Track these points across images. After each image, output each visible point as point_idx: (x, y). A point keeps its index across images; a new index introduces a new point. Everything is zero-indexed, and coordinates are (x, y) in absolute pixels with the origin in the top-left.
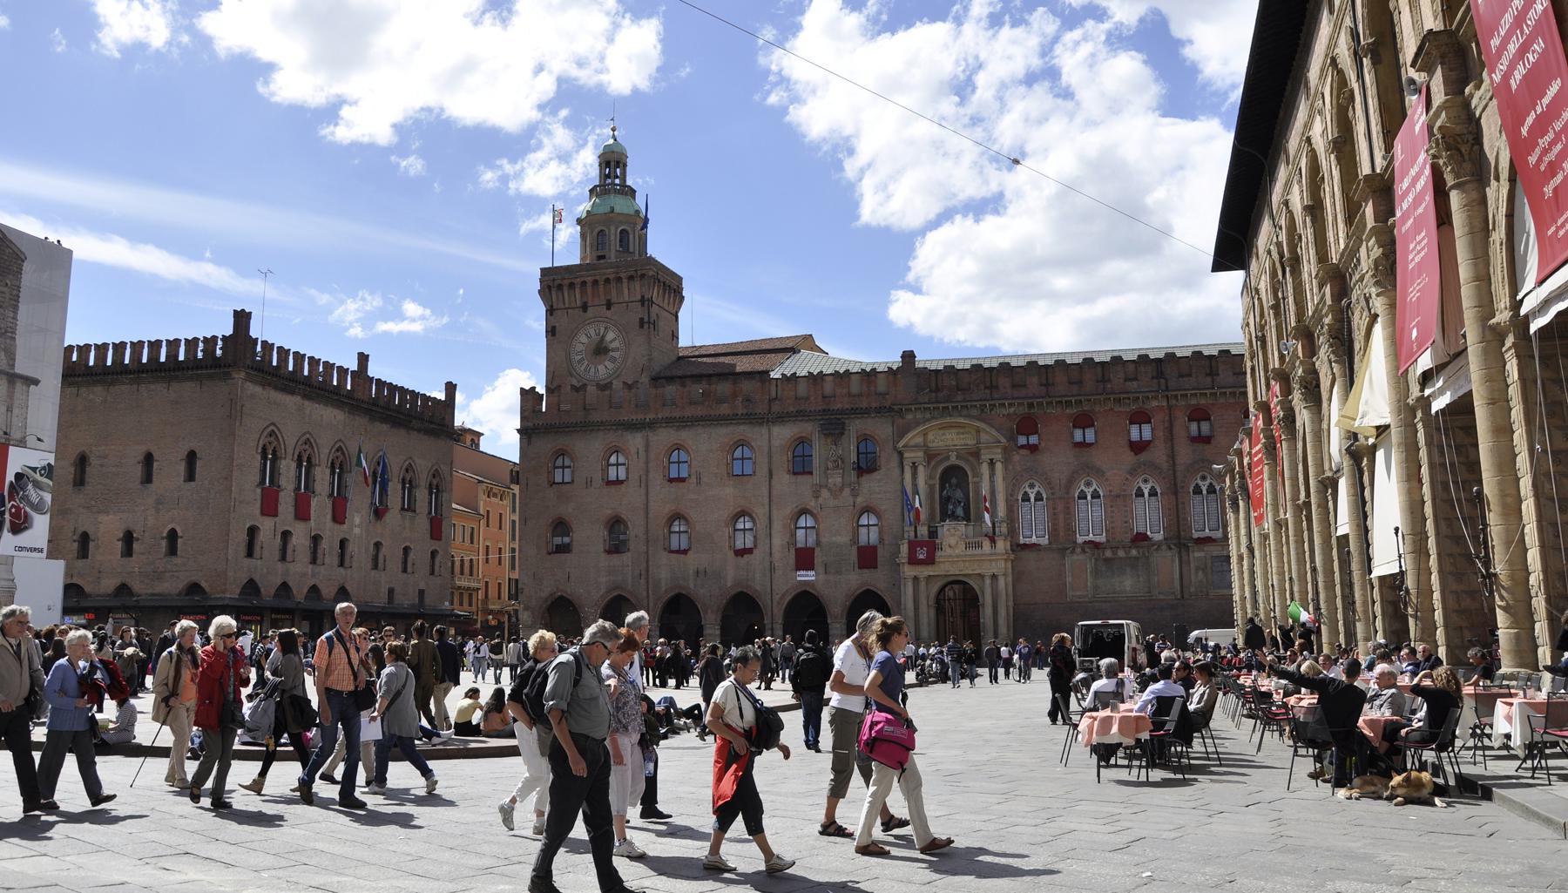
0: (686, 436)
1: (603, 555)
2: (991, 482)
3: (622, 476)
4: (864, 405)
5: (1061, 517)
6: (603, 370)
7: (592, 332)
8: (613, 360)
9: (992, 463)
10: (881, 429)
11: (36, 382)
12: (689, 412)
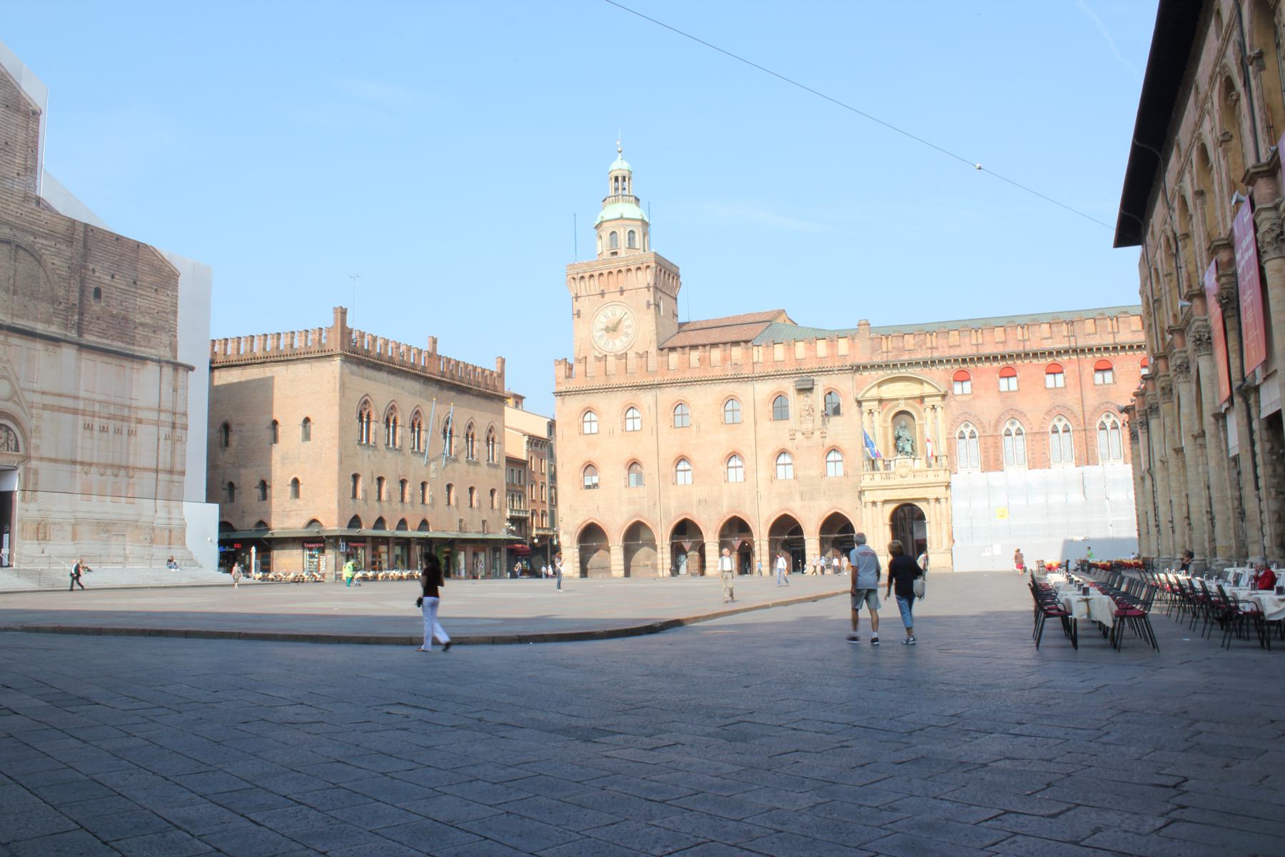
0: (687, 393)
2: (932, 426)
3: (638, 427)
4: (829, 364)
5: (991, 452)
6: (618, 344)
7: (609, 313)
8: (627, 335)
10: (846, 386)
11: (191, 369)
12: (688, 376)
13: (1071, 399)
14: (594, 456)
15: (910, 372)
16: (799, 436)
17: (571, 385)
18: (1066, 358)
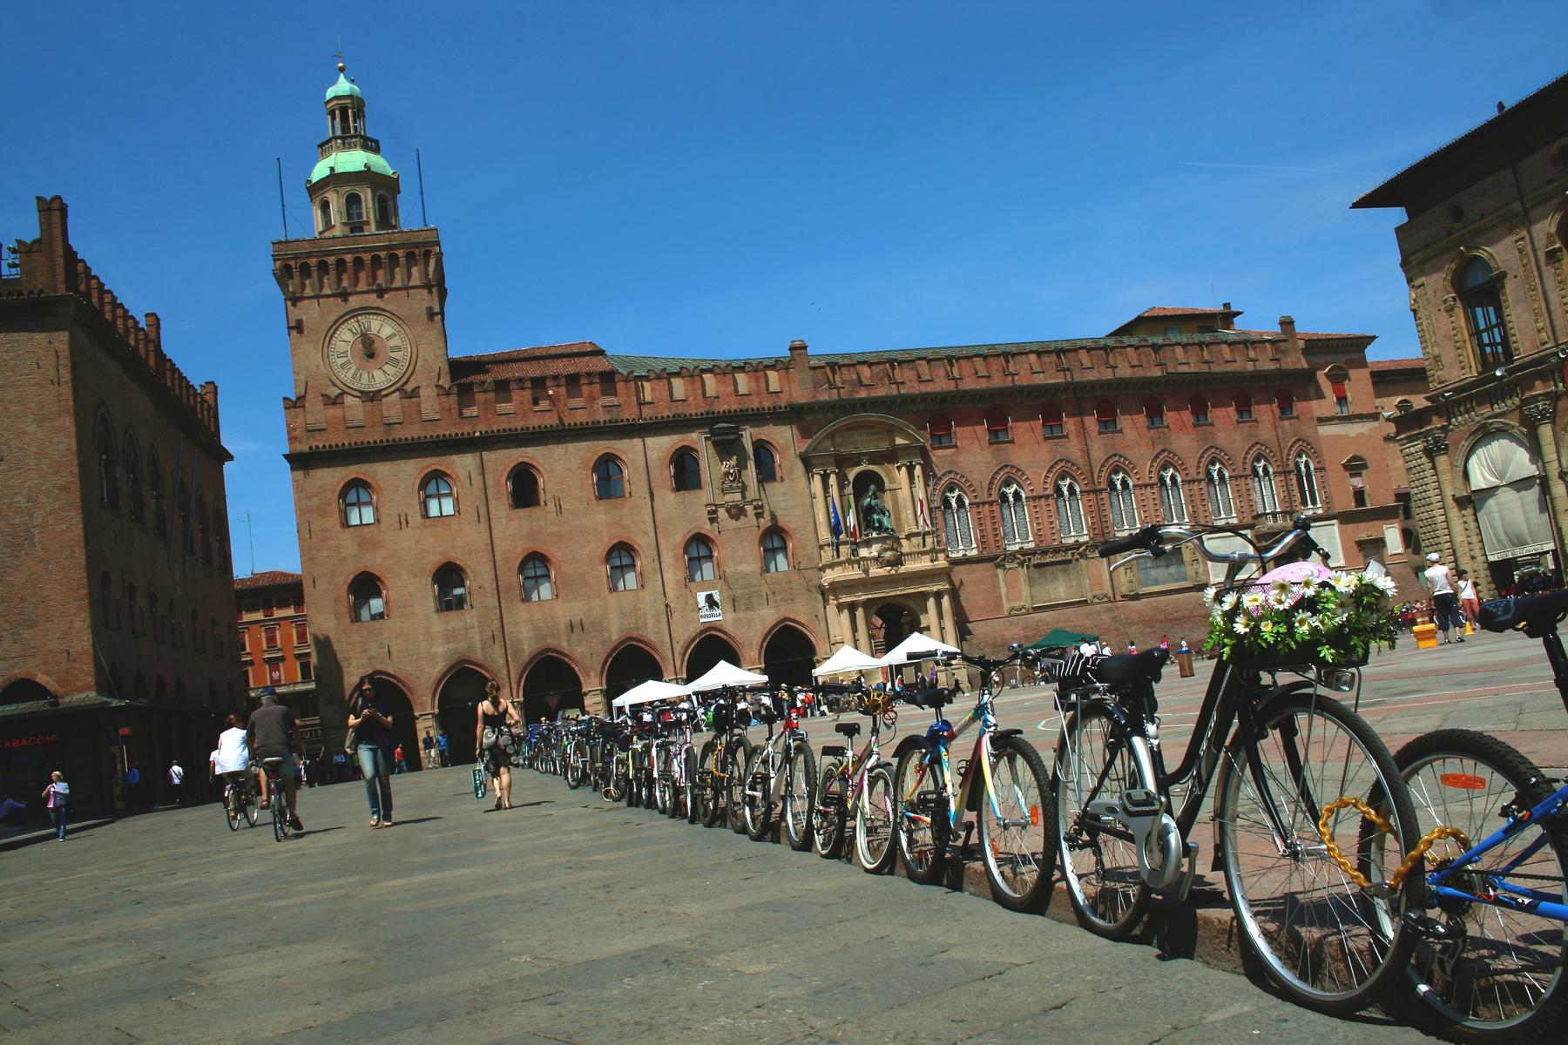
1: (435, 616)
4: (755, 405)
6: (380, 378)
8: (395, 362)
9: (910, 470)
13: (1073, 449)
14: (376, 562)
15: (873, 416)
16: (722, 513)
17: (320, 442)
18: (1063, 396)
